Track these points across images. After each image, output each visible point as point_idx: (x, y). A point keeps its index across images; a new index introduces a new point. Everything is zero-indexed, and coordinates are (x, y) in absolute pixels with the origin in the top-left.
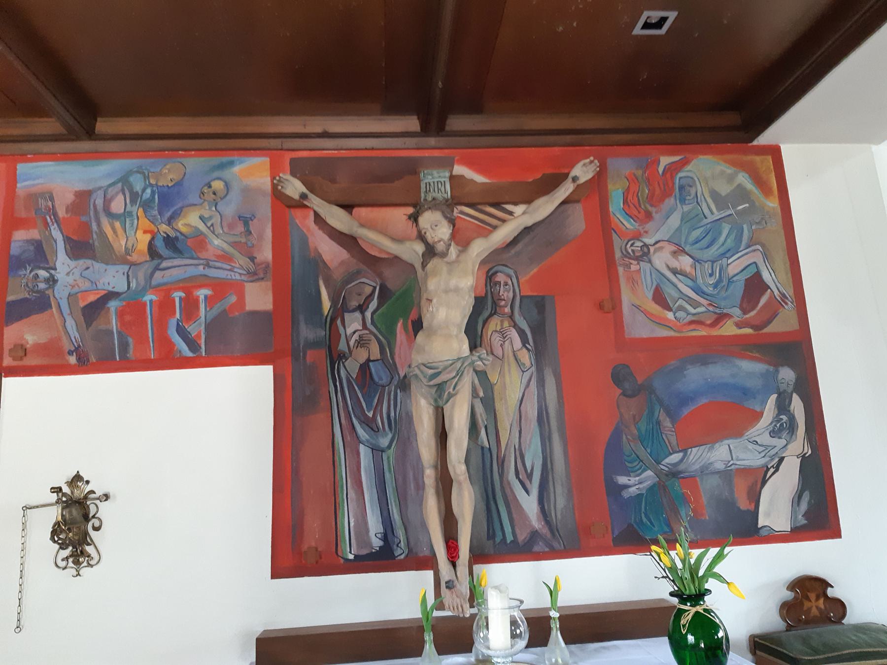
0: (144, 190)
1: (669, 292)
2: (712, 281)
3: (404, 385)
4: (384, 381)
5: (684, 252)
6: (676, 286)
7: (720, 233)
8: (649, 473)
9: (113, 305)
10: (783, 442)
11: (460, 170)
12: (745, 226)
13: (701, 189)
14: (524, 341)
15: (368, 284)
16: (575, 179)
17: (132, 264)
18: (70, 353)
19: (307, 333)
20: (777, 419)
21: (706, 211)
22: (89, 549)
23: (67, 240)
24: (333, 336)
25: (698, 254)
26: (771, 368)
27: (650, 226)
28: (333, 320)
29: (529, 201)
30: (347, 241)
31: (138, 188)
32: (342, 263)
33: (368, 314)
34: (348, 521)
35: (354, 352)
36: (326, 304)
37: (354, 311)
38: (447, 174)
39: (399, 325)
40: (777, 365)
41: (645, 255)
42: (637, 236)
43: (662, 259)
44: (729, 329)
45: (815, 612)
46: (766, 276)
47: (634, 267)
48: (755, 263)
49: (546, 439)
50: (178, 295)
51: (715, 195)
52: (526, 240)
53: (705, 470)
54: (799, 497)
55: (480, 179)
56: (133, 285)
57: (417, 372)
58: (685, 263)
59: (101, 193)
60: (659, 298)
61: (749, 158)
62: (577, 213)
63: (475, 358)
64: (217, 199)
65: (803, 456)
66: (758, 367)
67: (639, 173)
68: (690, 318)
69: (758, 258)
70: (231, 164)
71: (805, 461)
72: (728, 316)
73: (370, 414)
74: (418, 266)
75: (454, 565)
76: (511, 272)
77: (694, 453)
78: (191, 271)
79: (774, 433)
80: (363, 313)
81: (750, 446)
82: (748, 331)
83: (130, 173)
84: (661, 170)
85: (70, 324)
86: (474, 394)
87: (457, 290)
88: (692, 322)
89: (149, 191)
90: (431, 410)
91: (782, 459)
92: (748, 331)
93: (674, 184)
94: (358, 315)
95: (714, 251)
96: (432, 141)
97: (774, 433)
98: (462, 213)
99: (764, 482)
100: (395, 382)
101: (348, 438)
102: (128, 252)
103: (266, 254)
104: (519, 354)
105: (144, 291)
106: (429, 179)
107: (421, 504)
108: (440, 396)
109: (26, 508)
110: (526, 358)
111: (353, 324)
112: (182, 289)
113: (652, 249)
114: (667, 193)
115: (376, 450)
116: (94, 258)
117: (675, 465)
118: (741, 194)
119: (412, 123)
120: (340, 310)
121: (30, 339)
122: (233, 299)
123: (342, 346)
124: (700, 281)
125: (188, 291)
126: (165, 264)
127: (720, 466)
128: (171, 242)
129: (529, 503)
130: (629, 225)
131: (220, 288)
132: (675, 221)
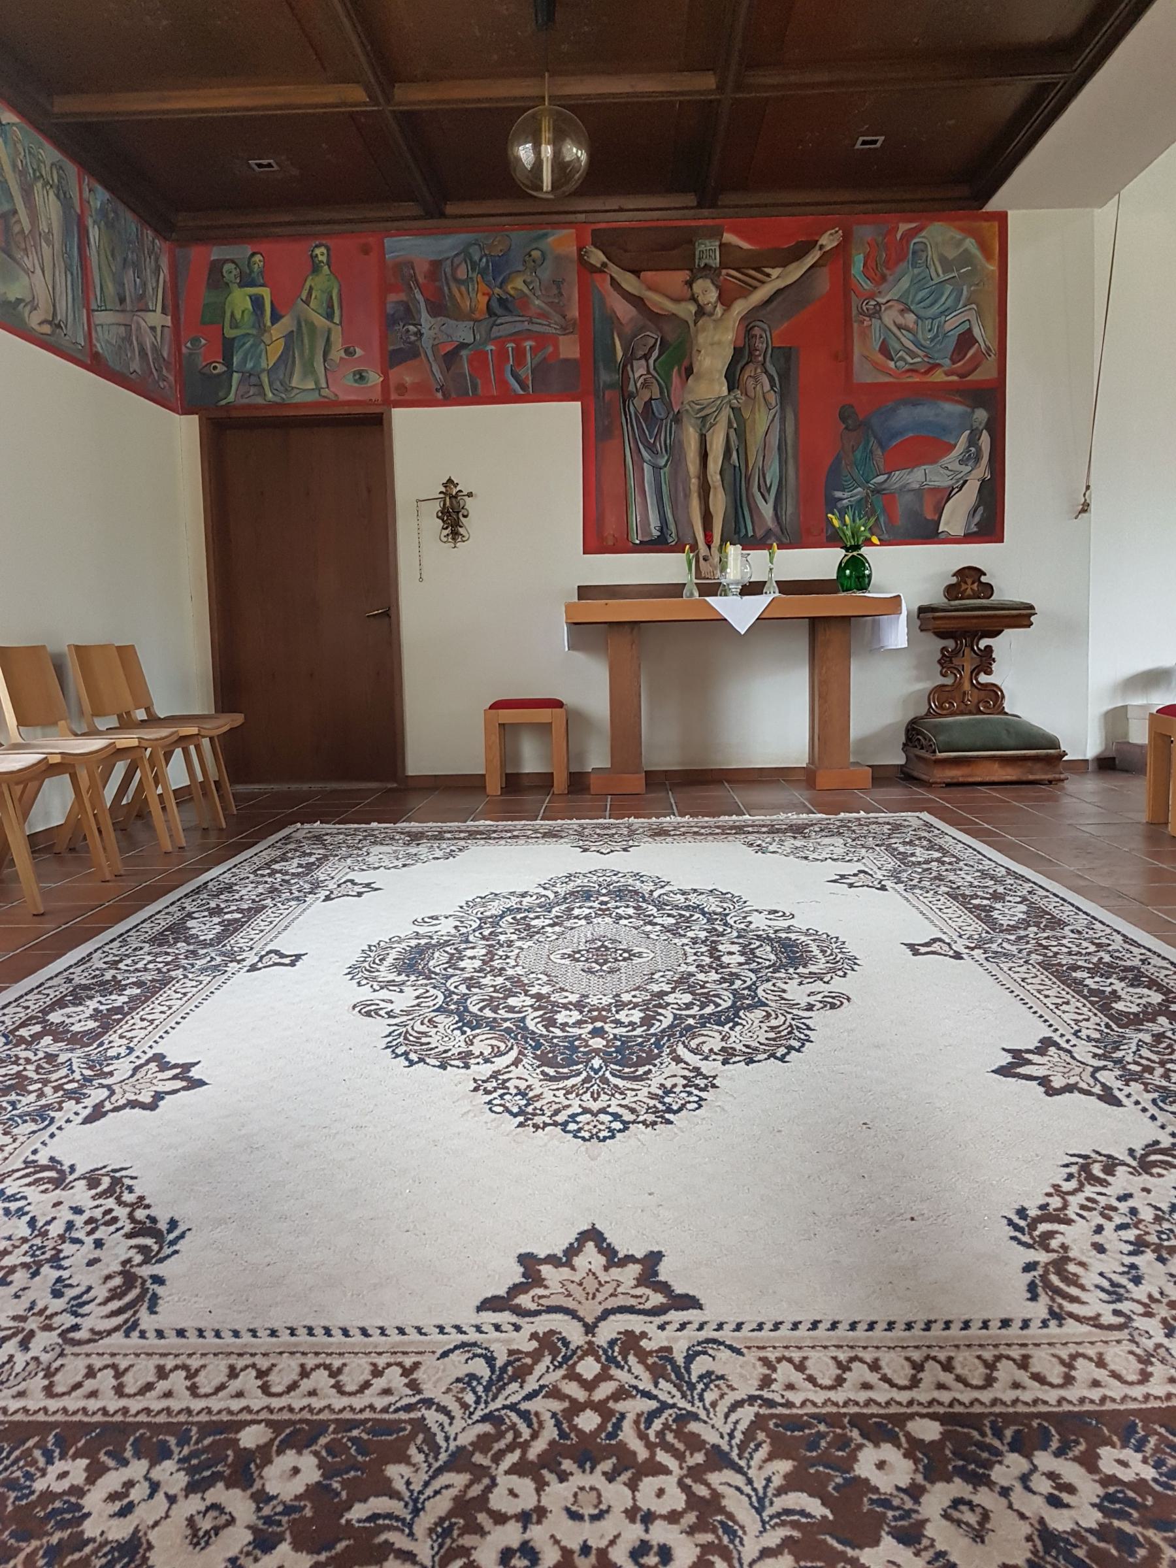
0: (481, 260)
3: (677, 419)
4: (663, 416)
6: (899, 339)
7: (942, 294)
9: (464, 353)
11: (729, 237)
12: (965, 288)
14: (772, 386)
15: (652, 336)
16: (821, 247)
17: (475, 321)
18: (437, 390)
19: (605, 377)
20: (967, 450)
21: (934, 275)
22: (461, 530)
23: (427, 301)
24: (625, 379)
25: (922, 313)
26: (969, 410)
27: (884, 286)
28: (625, 366)
29: (784, 265)
30: (637, 301)
31: (476, 258)
32: (631, 319)
33: (651, 362)
34: (635, 518)
35: (641, 392)
36: (620, 354)
37: (640, 359)
38: (717, 243)
39: (675, 370)
40: (974, 408)
41: (876, 313)
42: (872, 297)
43: (890, 317)
44: (938, 377)
45: (969, 592)
46: (977, 332)
49: (783, 463)
50: (510, 345)
51: (943, 260)
52: (780, 299)
53: (903, 489)
55: (745, 245)
56: (478, 337)
57: (688, 407)
58: (910, 318)
59: (449, 262)
60: (885, 350)
61: (977, 224)
62: (824, 274)
63: (731, 397)
64: (536, 265)
65: (983, 480)
66: (959, 408)
67: (880, 239)
68: (907, 367)
69: (972, 316)
70: (545, 235)
72: (939, 365)
73: (652, 441)
74: (691, 324)
75: (709, 547)
76: (766, 327)
78: (519, 327)
79: (961, 462)
80: (647, 361)
81: (942, 471)
82: (955, 378)
83: (470, 245)
84: (898, 236)
85: (435, 368)
86: (730, 425)
87: (719, 343)
88: (908, 371)
89: (484, 260)
90: (697, 436)
91: (966, 481)
92: (955, 378)
93: (908, 248)
94: (643, 362)
95: (935, 310)
96: (706, 212)
98: (728, 275)
100: (671, 416)
101: (635, 458)
102: (472, 311)
103: (575, 313)
104: (767, 396)
105: (485, 343)
106: (702, 247)
107: (688, 508)
108: (704, 426)
109: (418, 501)
110: (773, 398)
111: (639, 370)
112: (514, 341)
113: (883, 308)
114: (901, 258)
115: (656, 468)
116: (448, 317)
118: (966, 258)
119: (690, 199)
120: (629, 358)
121: (408, 380)
122: (550, 349)
123: (631, 388)
124: (920, 336)
125: (518, 343)
126: (499, 321)
127: (916, 486)
128: (501, 301)
129: (767, 510)
130: (867, 285)
131: (542, 340)
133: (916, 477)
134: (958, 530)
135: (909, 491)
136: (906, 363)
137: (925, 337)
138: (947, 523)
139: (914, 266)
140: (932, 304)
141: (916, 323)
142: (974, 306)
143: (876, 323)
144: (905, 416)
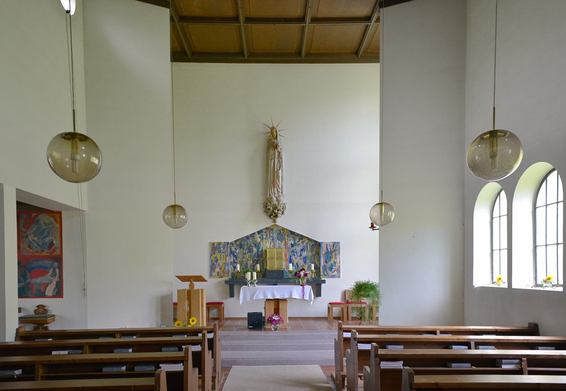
1: (32, 245)
2: (41, 243)
5: (36, 236)
7: (45, 232)
8: (23, 283)
10: (53, 278)
13: (41, 221)
21: (42, 227)
26: (53, 263)
27: (29, 230)
41: (27, 237)
42: (26, 232)
43: (31, 238)
44: (44, 254)
46: (54, 242)
47: (24, 239)
48: (52, 239)
51: (45, 223)
54: (55, 290)
58: (36, 239)
60: (29, 246)
71: (57, 283)
77: (33, 279)
84: (32, 217)
91: (52, 282)
95: (42, 236)
97: (52, 276)
99: (48, 286)
113: (29, 235)
117: (29, 282)
118: (51, 223)
124: (39, 243)
127: (39, 282)
130: (24, 230)
132: (34, 229)
133: (39, 280)
134: (51, 295)
135: (37, 284)
136: (35, 250)
137: (40, 243)
138: (47, 293)
139: (37, 225)
140: (42, 235)
141: (38, 239)
142: (53, 235)
143: (27, 239)
144: (35, 264)
